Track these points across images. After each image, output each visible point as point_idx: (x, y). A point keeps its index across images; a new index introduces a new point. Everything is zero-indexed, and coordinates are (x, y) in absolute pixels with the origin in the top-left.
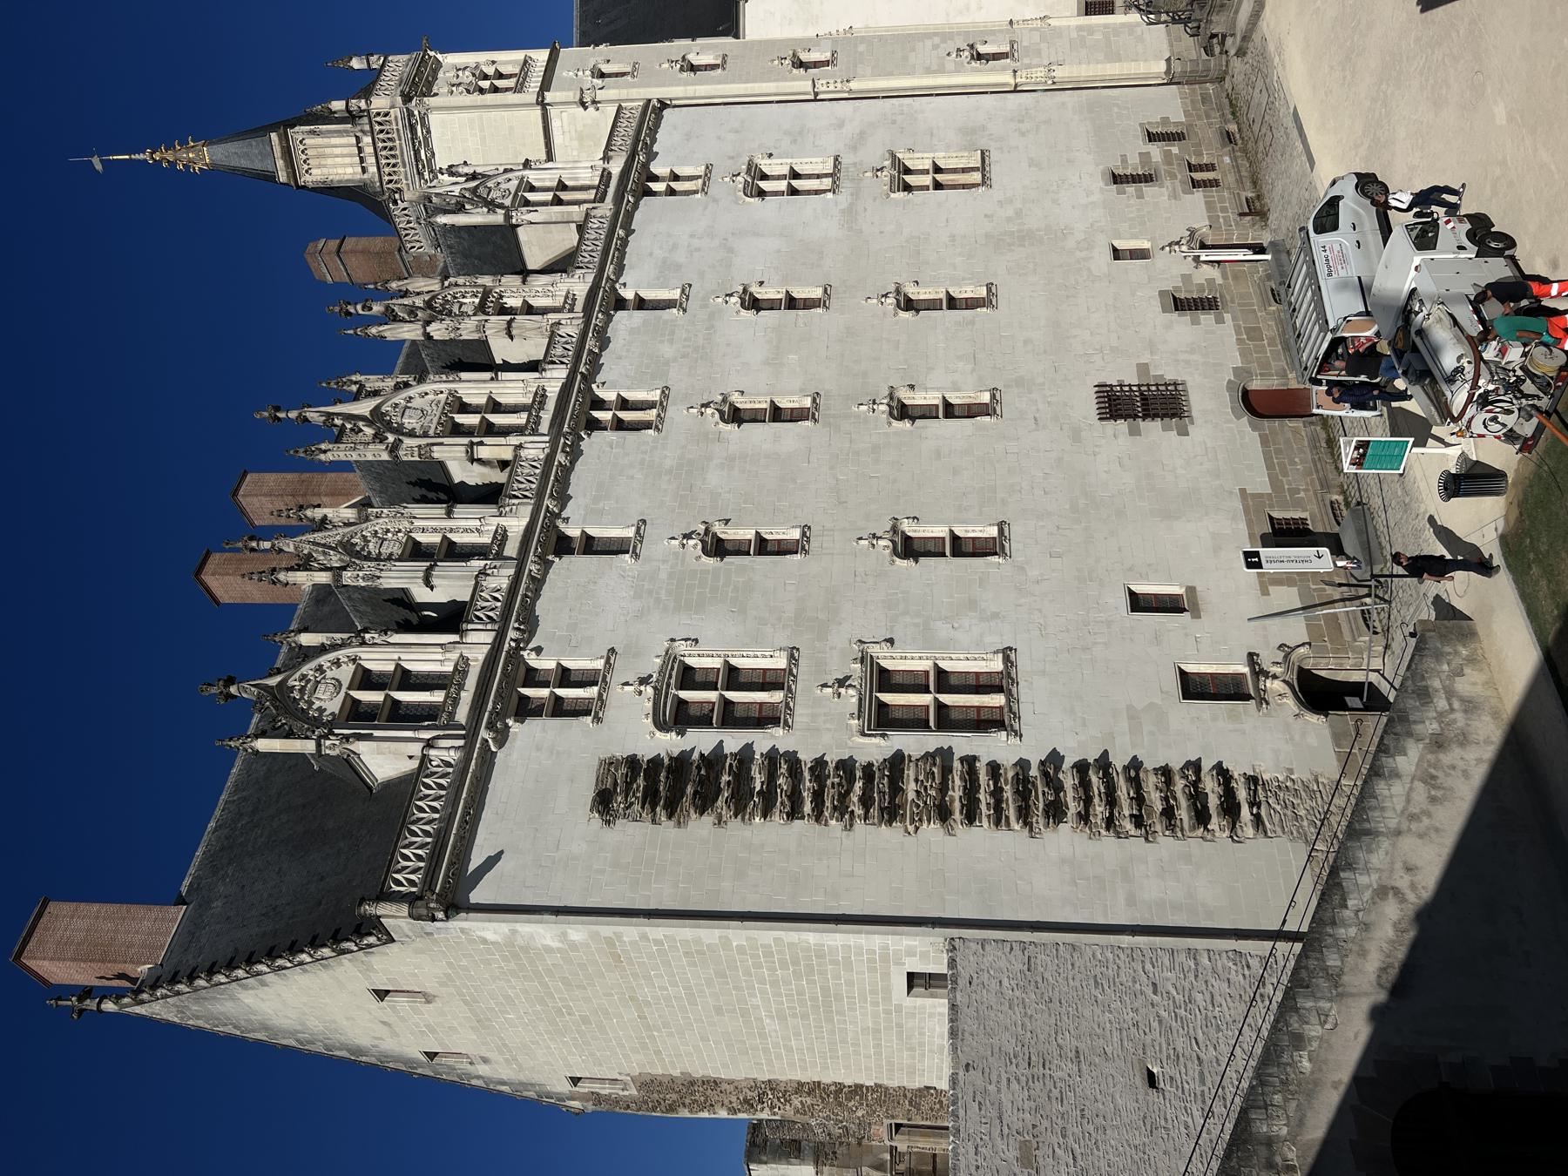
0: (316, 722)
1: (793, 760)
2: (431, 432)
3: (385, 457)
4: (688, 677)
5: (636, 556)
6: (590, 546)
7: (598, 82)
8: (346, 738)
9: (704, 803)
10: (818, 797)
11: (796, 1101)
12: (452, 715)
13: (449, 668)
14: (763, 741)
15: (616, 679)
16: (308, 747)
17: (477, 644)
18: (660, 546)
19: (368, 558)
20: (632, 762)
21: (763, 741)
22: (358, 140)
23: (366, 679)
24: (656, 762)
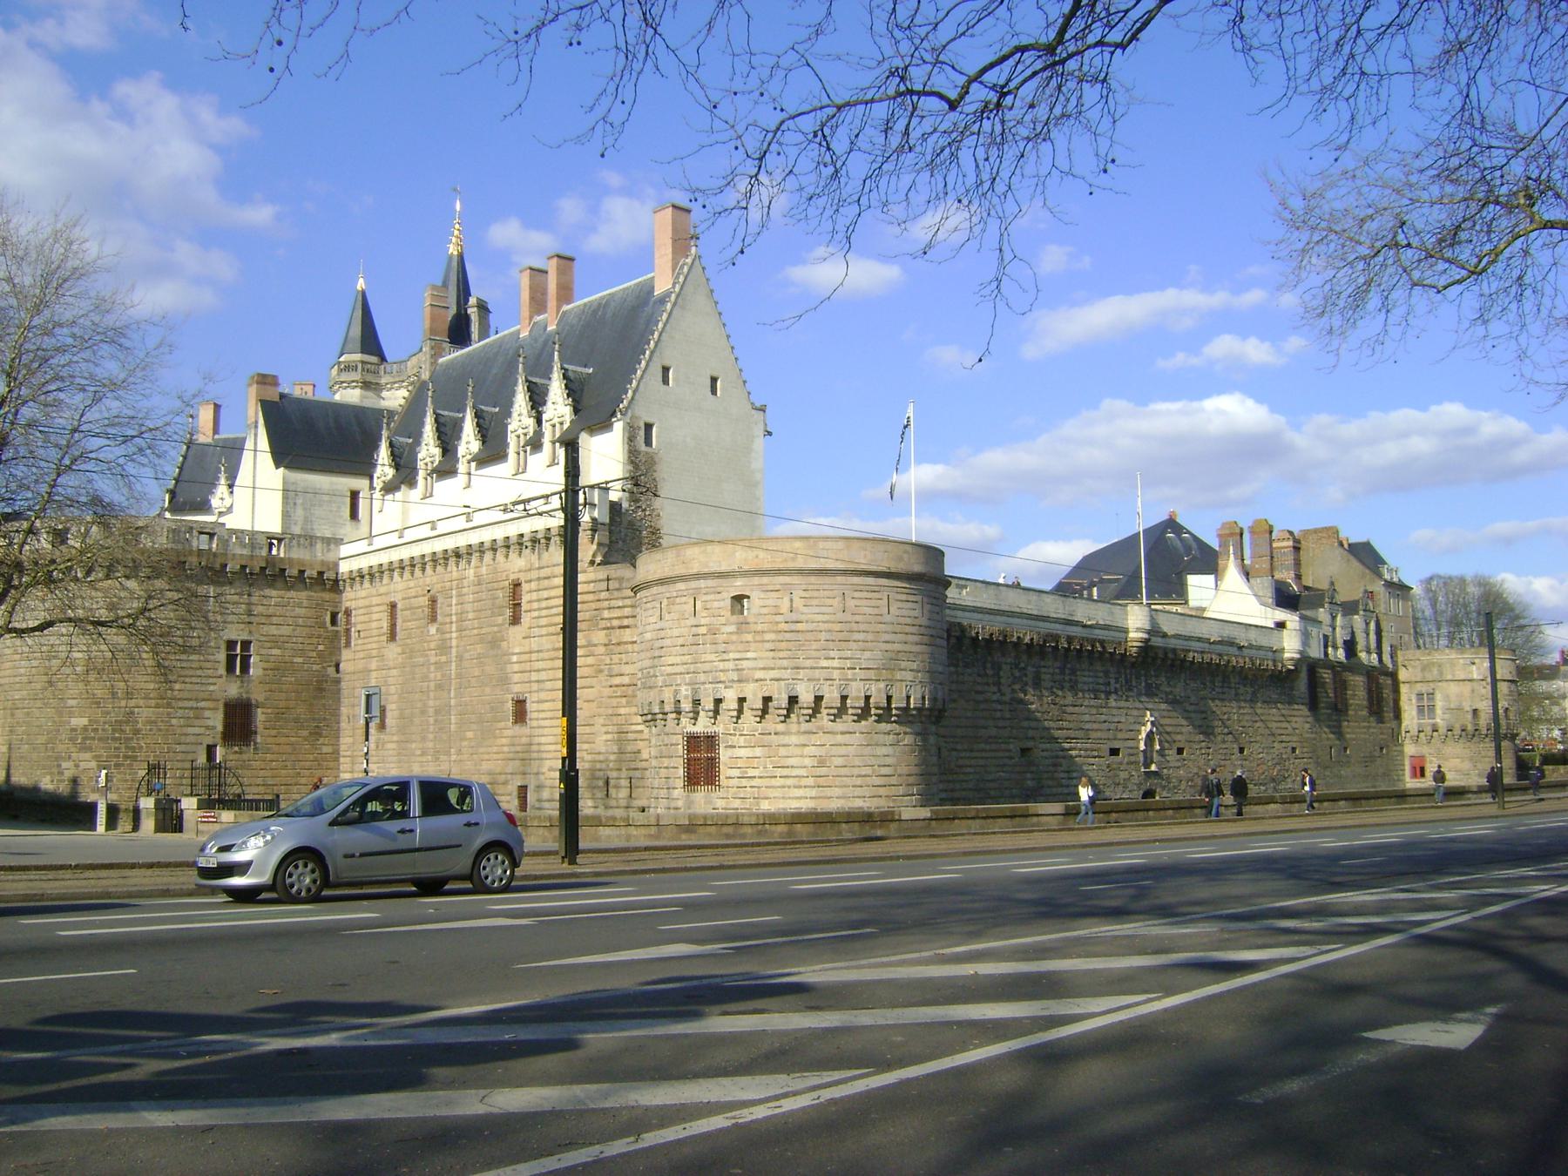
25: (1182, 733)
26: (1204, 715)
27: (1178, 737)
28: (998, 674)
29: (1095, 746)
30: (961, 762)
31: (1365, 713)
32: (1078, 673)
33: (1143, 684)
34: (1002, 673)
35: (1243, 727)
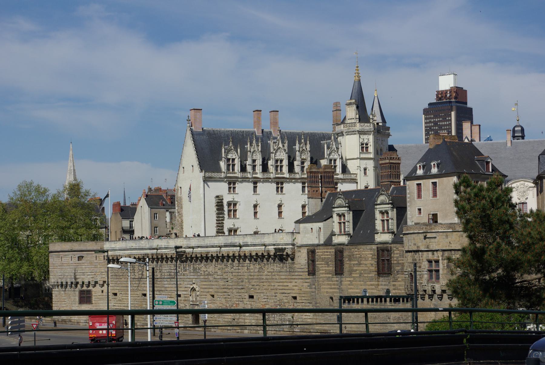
0: (227, 155)
1: (223, 220)
2: (276, 158)
3: (271, 151)
4: (235, 205)
5: (253, 194)
6: (255, 187)
7: (362, 169)
8: (225, 161)
9: (218, 209)
10: (219, 223)
11: (180, 219)
12: (228, 174)
13: (236, 171)
14: (226, 216)
15: (234, 195)
16: (223, 156)
17: (239, 175)
18: (255, 197)
19: (252, 154)
20: (223, 199)
21: (226, 216)
22: (353, 119)
23: (233, 160)
24: (222, 202)
25: (212, 288)
26: (226, 280)
27: (210, 290)
28: (134, 269)
29: (170, 294)
30: (123, 298)
31: (374, 274)
32: (163, 266)
33: (192, 268)
34: (135, 269)
35: (253, 285)
